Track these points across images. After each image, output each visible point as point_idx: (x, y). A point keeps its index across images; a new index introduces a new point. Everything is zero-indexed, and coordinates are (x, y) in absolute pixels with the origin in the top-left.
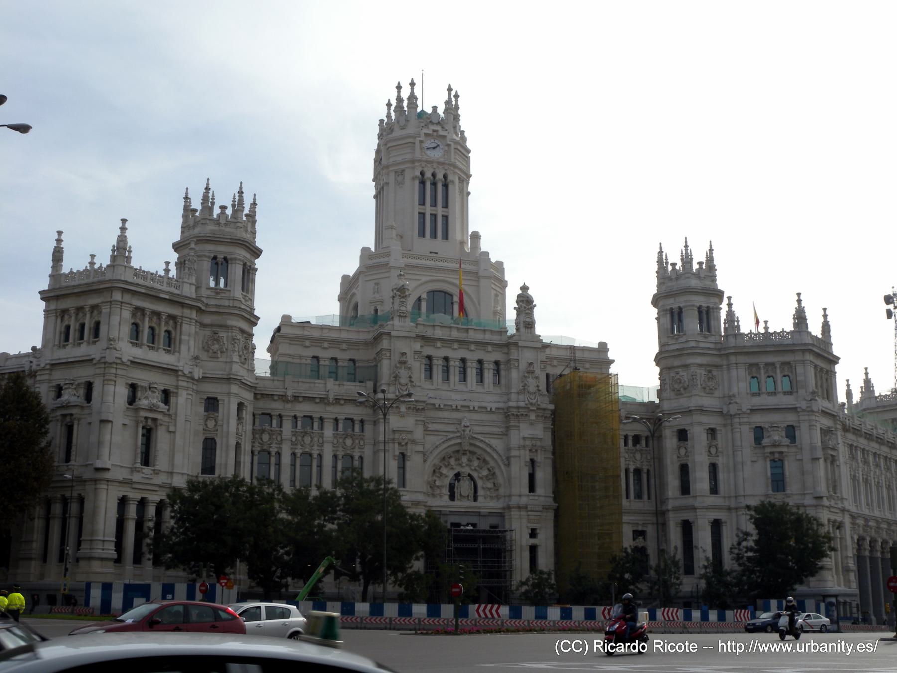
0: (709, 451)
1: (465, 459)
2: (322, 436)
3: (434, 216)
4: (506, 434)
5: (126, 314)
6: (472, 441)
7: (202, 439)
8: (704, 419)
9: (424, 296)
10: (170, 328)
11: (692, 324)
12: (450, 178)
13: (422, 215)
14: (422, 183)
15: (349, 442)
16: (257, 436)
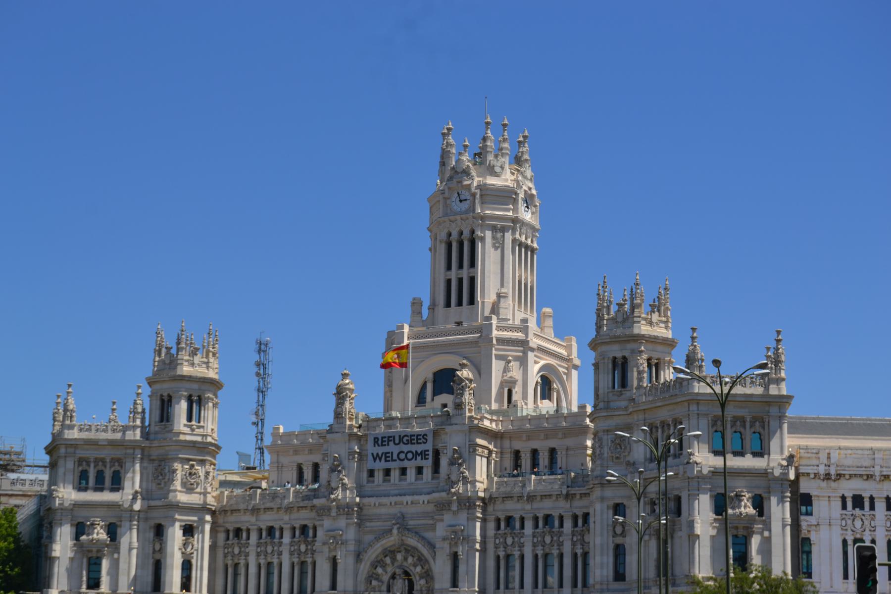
0: (615, 532)
1: (399, 557)
2: (280, 544)
3: (460, 281)
4: (433, 528)
5: (70, 464)
6: (404, 538)
7: (151, 561)
8: (609, 492)
9: (430, 376)
10: (117, 468)
11: (606, 380)
12: (476, 233)
13: (449, 282)
14: (449, 245)
15: (303, 548)
16: (230, 550)
